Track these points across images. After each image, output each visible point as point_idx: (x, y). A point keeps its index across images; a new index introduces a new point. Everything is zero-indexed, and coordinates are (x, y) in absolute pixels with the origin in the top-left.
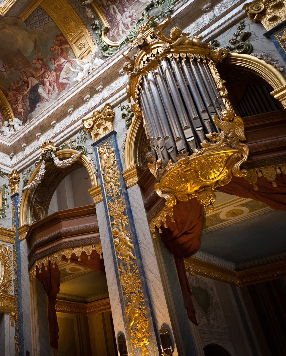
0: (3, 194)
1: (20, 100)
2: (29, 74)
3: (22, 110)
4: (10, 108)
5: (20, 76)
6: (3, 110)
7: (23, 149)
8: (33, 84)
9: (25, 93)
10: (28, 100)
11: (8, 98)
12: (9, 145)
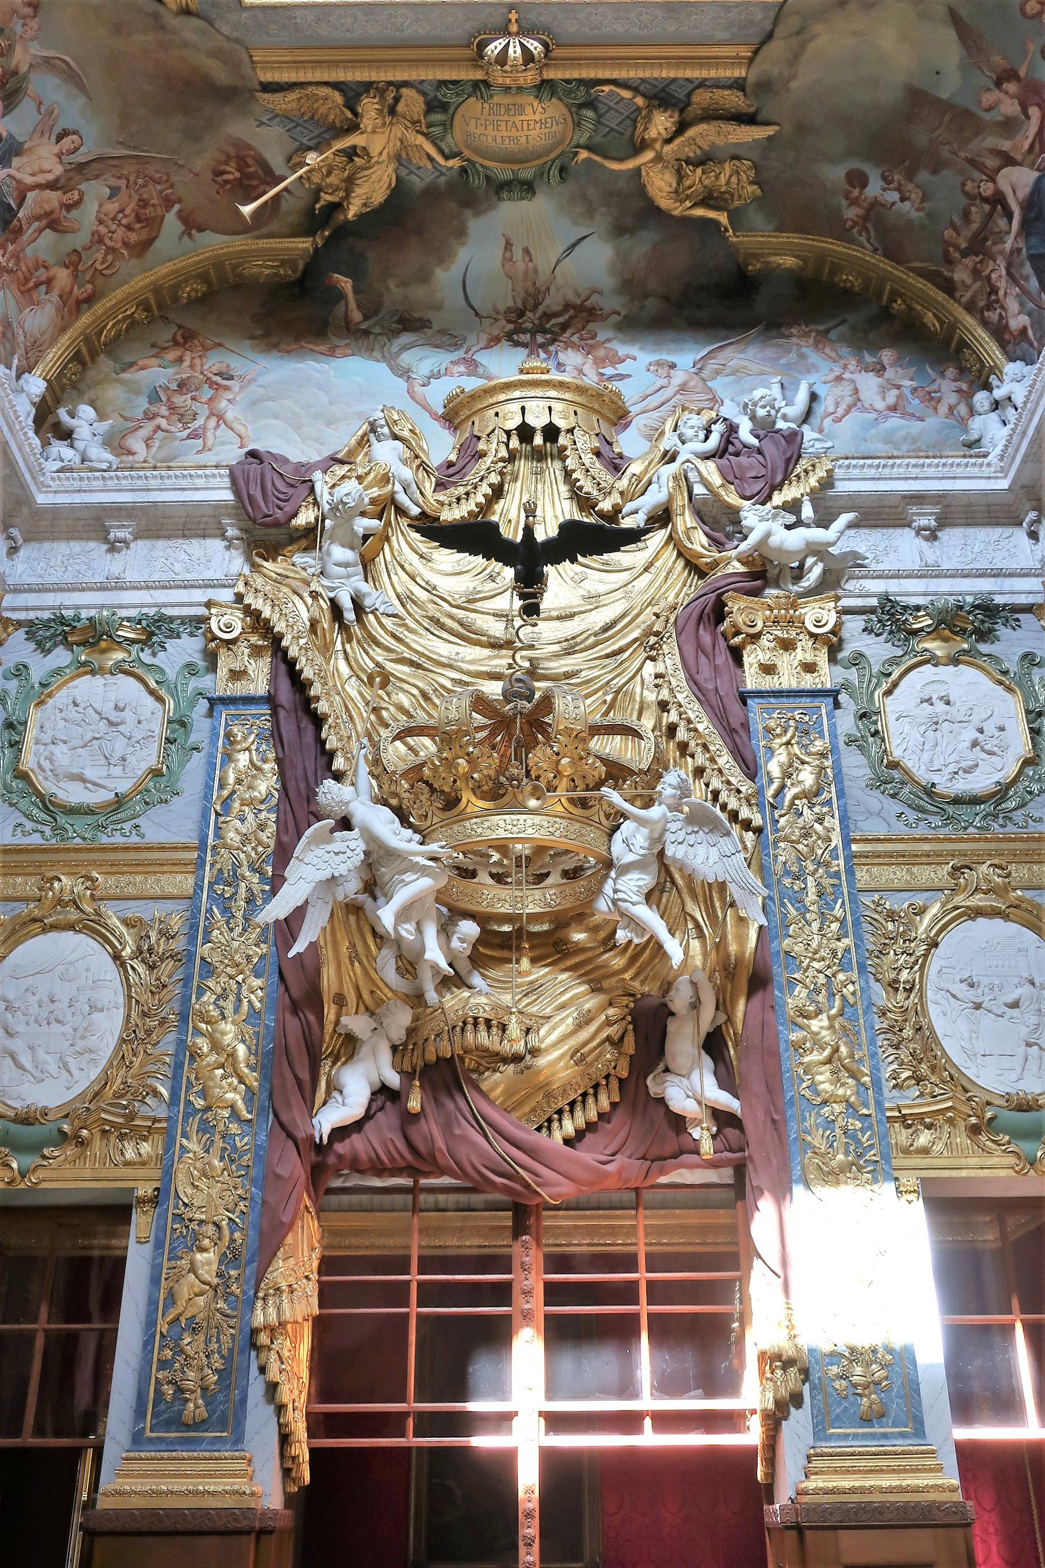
1: (1002, 284)
2: (991, 162)
3: (1023, 320)
4: (982, 333)
5: (963, 185)
6: (958, 350)
8: (1024, 192)
9: (1008, 245)
10: (1028, 269)
11: (957, 295)
12: (1004, 484)
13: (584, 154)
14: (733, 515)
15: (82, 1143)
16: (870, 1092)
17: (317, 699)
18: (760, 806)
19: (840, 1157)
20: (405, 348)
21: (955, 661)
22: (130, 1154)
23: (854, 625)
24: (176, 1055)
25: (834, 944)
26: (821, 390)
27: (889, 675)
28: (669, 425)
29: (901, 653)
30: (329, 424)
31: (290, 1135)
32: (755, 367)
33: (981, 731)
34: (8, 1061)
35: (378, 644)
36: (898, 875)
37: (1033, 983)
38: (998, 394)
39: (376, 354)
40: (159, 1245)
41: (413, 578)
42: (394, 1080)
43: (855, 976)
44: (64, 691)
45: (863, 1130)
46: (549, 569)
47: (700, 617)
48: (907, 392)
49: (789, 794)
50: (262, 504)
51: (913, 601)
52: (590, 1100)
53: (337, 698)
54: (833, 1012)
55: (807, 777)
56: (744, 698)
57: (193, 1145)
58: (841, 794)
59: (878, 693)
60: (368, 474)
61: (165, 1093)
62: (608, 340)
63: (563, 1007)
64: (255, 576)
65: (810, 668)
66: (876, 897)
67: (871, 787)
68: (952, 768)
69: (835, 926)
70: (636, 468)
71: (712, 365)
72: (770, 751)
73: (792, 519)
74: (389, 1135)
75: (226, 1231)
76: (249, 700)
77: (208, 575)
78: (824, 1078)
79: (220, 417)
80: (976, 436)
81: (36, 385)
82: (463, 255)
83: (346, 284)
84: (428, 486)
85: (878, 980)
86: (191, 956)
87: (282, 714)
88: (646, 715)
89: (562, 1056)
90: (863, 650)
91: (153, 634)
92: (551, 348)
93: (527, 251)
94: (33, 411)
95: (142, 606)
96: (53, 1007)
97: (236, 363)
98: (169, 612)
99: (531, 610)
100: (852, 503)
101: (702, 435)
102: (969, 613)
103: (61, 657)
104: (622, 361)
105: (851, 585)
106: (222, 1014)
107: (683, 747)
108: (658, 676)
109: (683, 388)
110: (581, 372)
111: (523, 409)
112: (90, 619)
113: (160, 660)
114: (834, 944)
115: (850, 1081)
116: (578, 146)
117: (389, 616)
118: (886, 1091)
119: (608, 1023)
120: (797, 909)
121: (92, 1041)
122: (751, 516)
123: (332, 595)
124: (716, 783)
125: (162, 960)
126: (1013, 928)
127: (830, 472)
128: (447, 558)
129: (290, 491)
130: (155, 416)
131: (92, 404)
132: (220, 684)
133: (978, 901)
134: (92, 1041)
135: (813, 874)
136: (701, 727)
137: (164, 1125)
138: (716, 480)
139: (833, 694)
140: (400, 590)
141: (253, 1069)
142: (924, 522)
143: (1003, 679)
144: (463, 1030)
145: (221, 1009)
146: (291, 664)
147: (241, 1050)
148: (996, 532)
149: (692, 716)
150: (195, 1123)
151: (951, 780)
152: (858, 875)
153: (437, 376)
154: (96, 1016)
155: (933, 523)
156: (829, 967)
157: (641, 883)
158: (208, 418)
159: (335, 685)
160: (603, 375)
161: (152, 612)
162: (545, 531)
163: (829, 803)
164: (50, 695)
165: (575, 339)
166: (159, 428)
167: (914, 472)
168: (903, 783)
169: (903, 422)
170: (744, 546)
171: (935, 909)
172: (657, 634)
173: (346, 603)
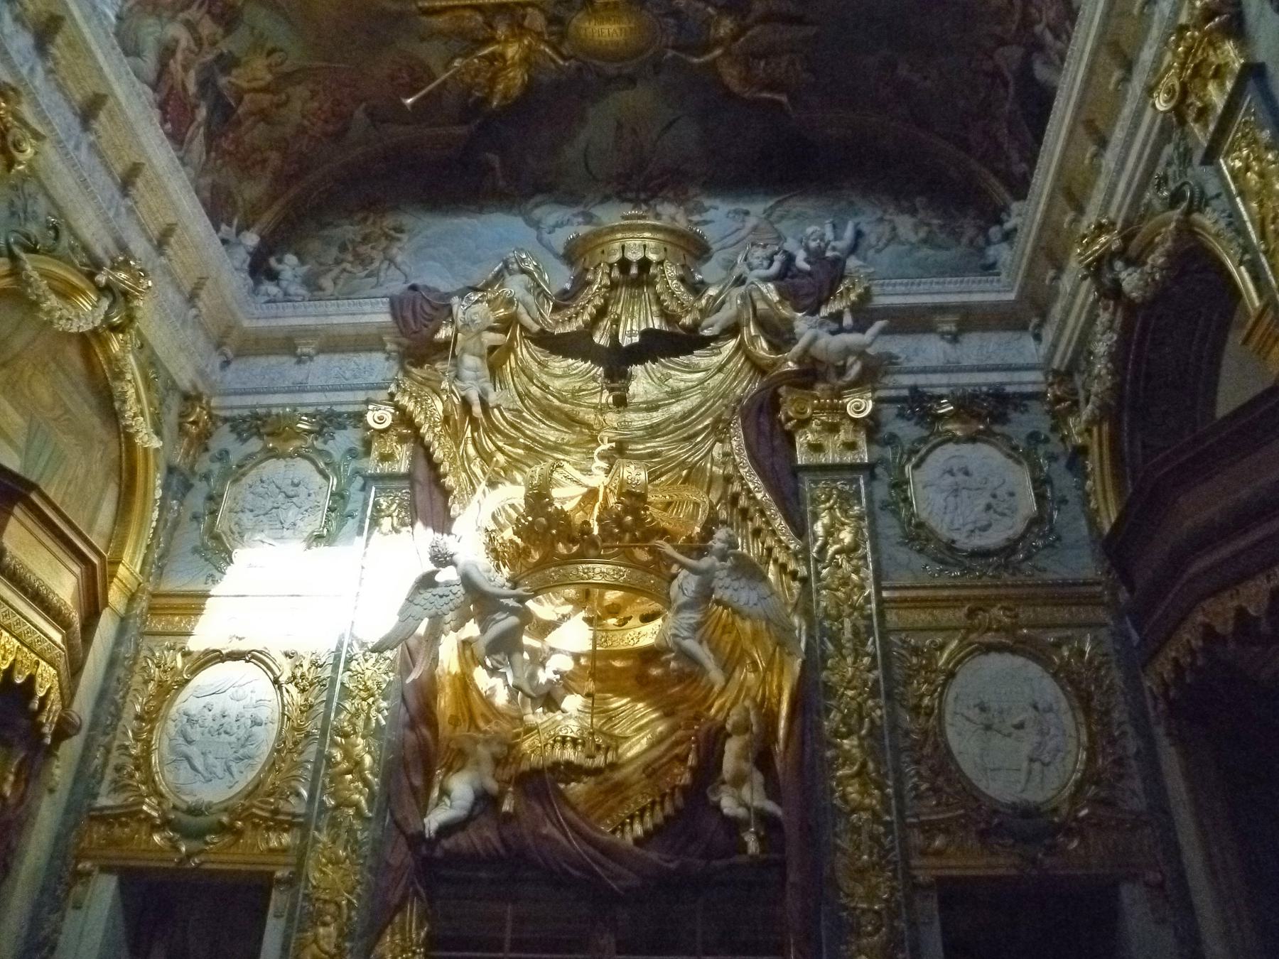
0: (1035, 467)
4: (993, 181)
7: (1053, 294)
12: (1012, 296)
13: (670, 53)
14: (789, 322)
15: (239, 833)
16: (893, 802)
17: (445, 475)
18: (806, 561)
19: (865, 857)
20: (537, 206)
21: (972, 439)
22: (274, 844)
23: (890, 411)
24: (315, 763)
25: (865, 675)
26: (865, 228)
27: (918, 451)
28: (740, 259)
29: (926, 433)
30: (474, 263)
31: (403, 833)
32: (811, 212)
33: (994, 496)
34: (186, 764)
35: (500, 432)
36: (921, 617)
37: (1035, 707)
38: (1008, 225)
39: (515, 211)
40: (290, 919)
41: (531, 380)
42: (492, 786)
43: (882, 702)
44: (254, 472)
45: (886, 835)
46: (637, 370)
47: (760, 410)
48: (936, 229)
49: (831, 550)
50: (412, 322)
51: (938, 391)
52: (658, 808)
53: (464, 475)
54: (864, 732)
55: (846, 536)
56: (796, 471)
57: (324, 837)
58: (875, 550)
59: (908, 468)
60: (496, 298)
61: (305, 794)
62: (696, 196)
63: (641, 729)
64: (406, 379)
65: (851, 446)
66: (903, 635)
67: (902, 544)
68: (970, 527)
69: (866, 660)
70: (712, 292)
71: (779, 212)
72: (816, 517)
73: (834, 326)
74: (488, 834)
75: (345, 911)
76: (393, 477)
77: (372, 379)
78: (853, 791)
79: (392, 261)
80: (991, 260)
81: (251, 239)
82: (582, 137)
83: (494, 159)
84: (548, 308)
85: (902, 706)
86: (333, 681)
87: (418, 488)
88: (715, 486)
89: (636, 770)
90: (896, 431)
91: (324, 426)
92: (652, 202)
93: (634, 131)
94: (249, 260)
95: (318, 404)
96: (224, 720)
97: (407, 220)
98: (337, 409)
99: (621, 403)
100: (886, 312)
101: (766, 263)
102: (984, 400)
103: (255, 445)
104: (706, 210)
105: (888, 380)
106: (354, 729)
107: (744, 513)
108: (726, 455)
109: (755, 229)
110: (673, 219)
111: (623, 247)
112: (278, 415)
113: (330, 446)
114: (865, 675)
115: (876, 792)
116: (667, 47)
117: (509, 410)
118: (907, 800)
119: (677, 743)
120: (835, 646)
121: (250, 749)
122: (803, 325)
123: (463, 393)
124: (770, 542)
125: (311, 685)
126: (1019, 661)
127: (867, 290)
128: (558, 364)
129: (434, 313)
130: (343, 261)
131: (297, 254)
132: (372, 465)
133: (989, 637)
134: (250, 749)
135: (849, 616)
136: (759, 496)
137: (301, 820)
138: (775, 297)
139: (869, 469)
140: (520, 389)
141: (375, 775)
142: (946, 328)
143: (1013, 452)
144: (553, 747)
145: (354, 725)
146: (426, 448)
147: (368, 760)
148: (1007, 336)
149: (752, 486)
150: (325, 820)
151: (968, 537)
152: (888, 617)
153: (559, 225)
154: (256, 729)
155: (954, 329)
156: (860, 694)
157: (692, 621)
158: (382, 262)
159: (463, 465)
160: (690, 221)
161: (325, 409)
162: (629, 335)
163: (864, 557)
164: (244, 475)
165: (671, 195)
166: (344, 270)
167: (936, 288)
168: (928, 540)
169: (931, 252)
170: (797, 349)
171: (954, 644)
172: (725, 421)
173: (474, 396)
